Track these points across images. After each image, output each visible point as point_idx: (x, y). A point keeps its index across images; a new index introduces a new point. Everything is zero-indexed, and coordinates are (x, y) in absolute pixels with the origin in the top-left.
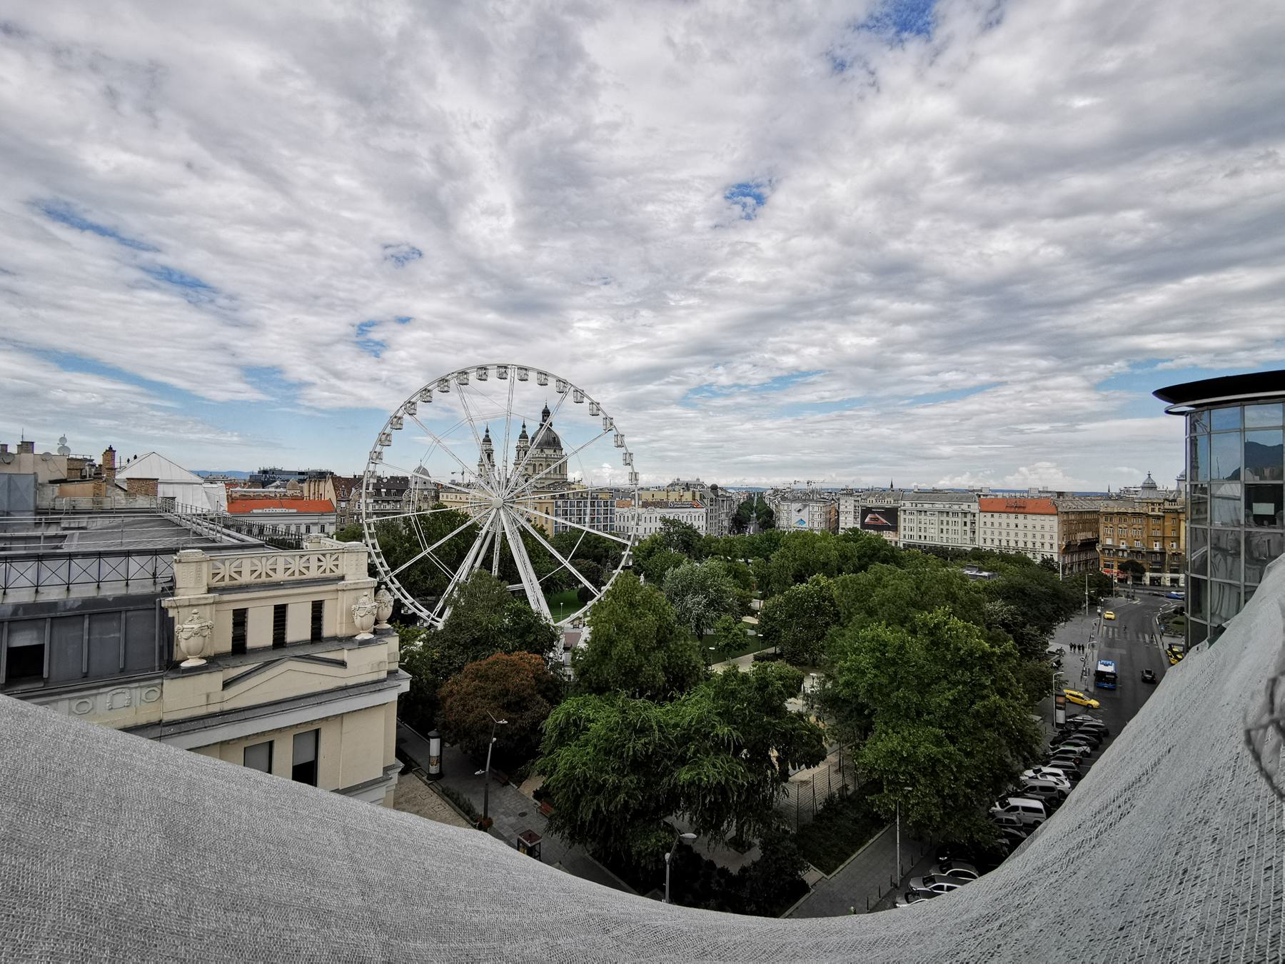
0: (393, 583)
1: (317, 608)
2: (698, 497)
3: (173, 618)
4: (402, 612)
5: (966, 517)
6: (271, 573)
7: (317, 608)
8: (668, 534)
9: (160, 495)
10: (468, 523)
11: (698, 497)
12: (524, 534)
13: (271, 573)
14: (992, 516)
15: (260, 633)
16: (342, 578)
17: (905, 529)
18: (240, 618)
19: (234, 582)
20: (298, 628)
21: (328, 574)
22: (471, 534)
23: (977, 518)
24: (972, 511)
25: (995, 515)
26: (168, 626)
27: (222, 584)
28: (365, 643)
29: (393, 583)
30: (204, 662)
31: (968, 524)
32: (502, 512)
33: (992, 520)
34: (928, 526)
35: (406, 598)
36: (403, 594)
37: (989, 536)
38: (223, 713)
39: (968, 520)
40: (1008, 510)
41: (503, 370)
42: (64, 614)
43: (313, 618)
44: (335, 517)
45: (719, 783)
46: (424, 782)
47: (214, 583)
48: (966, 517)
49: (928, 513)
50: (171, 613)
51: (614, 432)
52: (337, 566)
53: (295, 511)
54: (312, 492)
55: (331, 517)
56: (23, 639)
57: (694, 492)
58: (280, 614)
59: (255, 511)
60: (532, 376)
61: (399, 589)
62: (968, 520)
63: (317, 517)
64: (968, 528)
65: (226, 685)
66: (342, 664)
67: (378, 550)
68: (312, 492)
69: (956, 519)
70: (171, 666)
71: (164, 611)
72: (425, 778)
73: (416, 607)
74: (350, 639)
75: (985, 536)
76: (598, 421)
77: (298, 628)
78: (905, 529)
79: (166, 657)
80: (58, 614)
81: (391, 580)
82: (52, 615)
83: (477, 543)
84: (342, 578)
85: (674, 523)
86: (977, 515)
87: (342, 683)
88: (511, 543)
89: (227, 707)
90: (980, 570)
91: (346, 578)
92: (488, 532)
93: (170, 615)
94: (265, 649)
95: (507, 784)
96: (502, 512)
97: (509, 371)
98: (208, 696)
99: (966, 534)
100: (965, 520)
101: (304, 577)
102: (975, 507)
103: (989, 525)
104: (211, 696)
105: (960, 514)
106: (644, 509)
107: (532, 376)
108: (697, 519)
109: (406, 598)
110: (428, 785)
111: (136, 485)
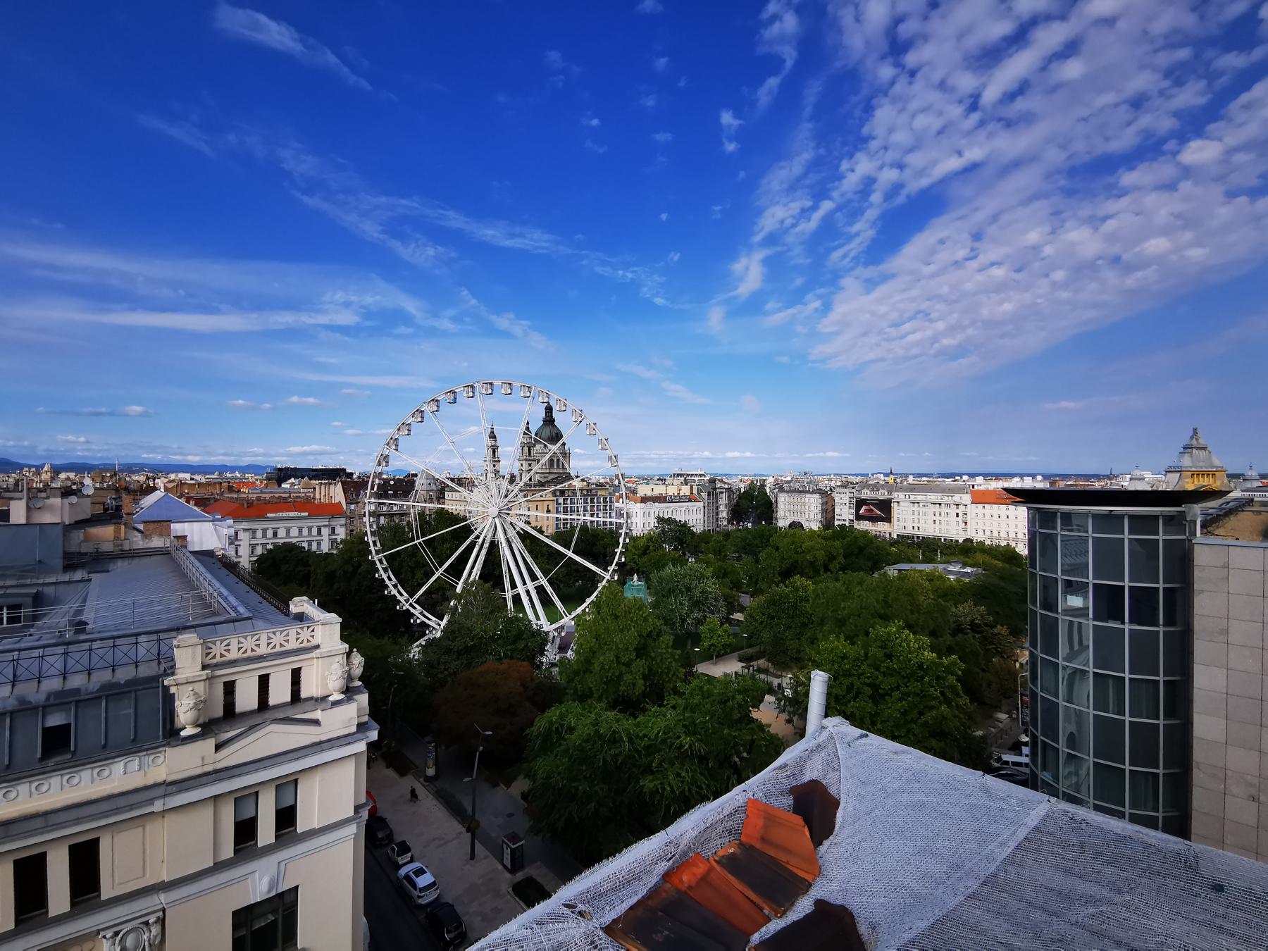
1: (296, 675)
2: (695, 491)
3: (174, 694)
6: (255, 648)
7: (296, 675)
8: (663, 532)
9: (173, 534)
11: (695, 491)
13: (255, 648)
14: (984, 507)
15: (247, 698)
16: (318, 647)
17: (898, 521)
18: (230, 688)
19: (223, 659)
20: (280, 693)
21: (305, 644)
26: (169, 700)
27: (214, 661)
28: (336, 703)
30: (199, 730)
32: (497, 520)
33: (984, 511)
34: (920, 517)
38: (216, 772)
40: (1000, 501)
42: (87, 697)
43: (293, 684)
45: (682, 792)
46: (421, 783)
47: (208, 661)
49: (921, 504)
50: (173, 690)
52: (313, 636)
53: (306, 514)
54: (323, 494)
56: (55, 720)
57: (692, 487)
58: (264, 681)
59: (269, 515)
63: (328, 520)
64: (960, 519)
65: (218, 747)
66: (316, 722)
68: (323, 494)
69: (948, 511)
70: (172, 734)
71: (166, 689)
72: (422, 780)
74: (324, 698)
77: (280, 693)
78: (898, 521)
79: (168, 727)
80: (82, 698)
82: (77, 698)
84: (318, 647)
85: (670, 521)
87: (317, 739)
89: (219, 766)
91: (321, 646)
93: (172, 692)
94: (251, 713)
95: (496, 785)
98: (203, 759)
99: (958, 525)
101: (283, 649)
102: (967, 498)
103: (980, 515)
104: (205, 758)
108: (694, 516)
110: (424, 786)
111: (152, 526)
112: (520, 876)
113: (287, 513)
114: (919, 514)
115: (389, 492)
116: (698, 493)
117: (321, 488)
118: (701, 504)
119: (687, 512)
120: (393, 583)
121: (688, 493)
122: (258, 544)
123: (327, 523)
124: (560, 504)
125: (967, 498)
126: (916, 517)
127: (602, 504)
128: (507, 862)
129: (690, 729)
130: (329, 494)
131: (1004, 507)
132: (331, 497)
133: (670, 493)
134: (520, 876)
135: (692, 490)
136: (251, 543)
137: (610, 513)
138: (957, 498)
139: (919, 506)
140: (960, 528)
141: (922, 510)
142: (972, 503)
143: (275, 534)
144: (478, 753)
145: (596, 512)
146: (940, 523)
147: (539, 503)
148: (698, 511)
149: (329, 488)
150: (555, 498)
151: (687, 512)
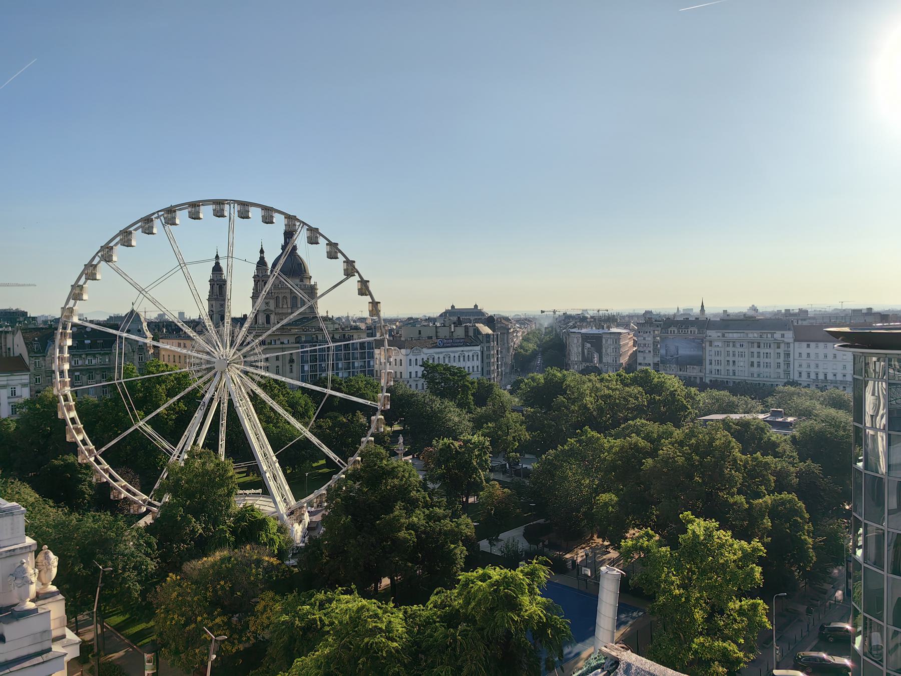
0: (99, 463)
4: (112, 497)
5: (779, 347)
10: (187, 390)
12: (254, 397)
14: (808, 346)
17: (711, 364)
22: (193, 400)
24: (786, 340)
25: (812, 345)
29: (99, 463)
31: (782, 355)
33: (808, 351)
34: (736, 359)
35: (116, 480)
36: (111, 476)
37: (804, 370)
39: (781, 351)
41: (218, 207)
44: (27, 377)
48: (779, 347)
49: (738, 345)
51: (356, 278)
55: (23, 377)
60: (256, 214)
61: (106, 471)
62: (781, 351)
63: (5, 378)
64: (781, 360)
67: (81, 426)
73: (128, 491)
75: (800, 369)
76: (339, 265)
78: (711, 364)
81: (96, 460)
83: (198, 415)
86: (792, 345)
88: (241, 411)
92: (212, 399)
97: (227, 207)
99: (779, 367)
100: (778, 351)
102: (789, 336)
103: (804, 356)
105: (772, 345)
106: (409, 351)
107: (256, 214)
109: (116, 480)
114: (734, 355)
115: (86, 342)
118: (478, 348)
119: (462, 359)
123: (5, 383)
126: (731, 359)
130: (5, 345)
132: (9, 349)
137: (369, 362)
138: (778, 335)
139: (734, 346)
140: (781, 371)
141: (739, 349)
142: (795, 341)
144: (210, 663)
146: (759, 366)
148: (475, 358)
149: (5, 338)
151: (462, 359)
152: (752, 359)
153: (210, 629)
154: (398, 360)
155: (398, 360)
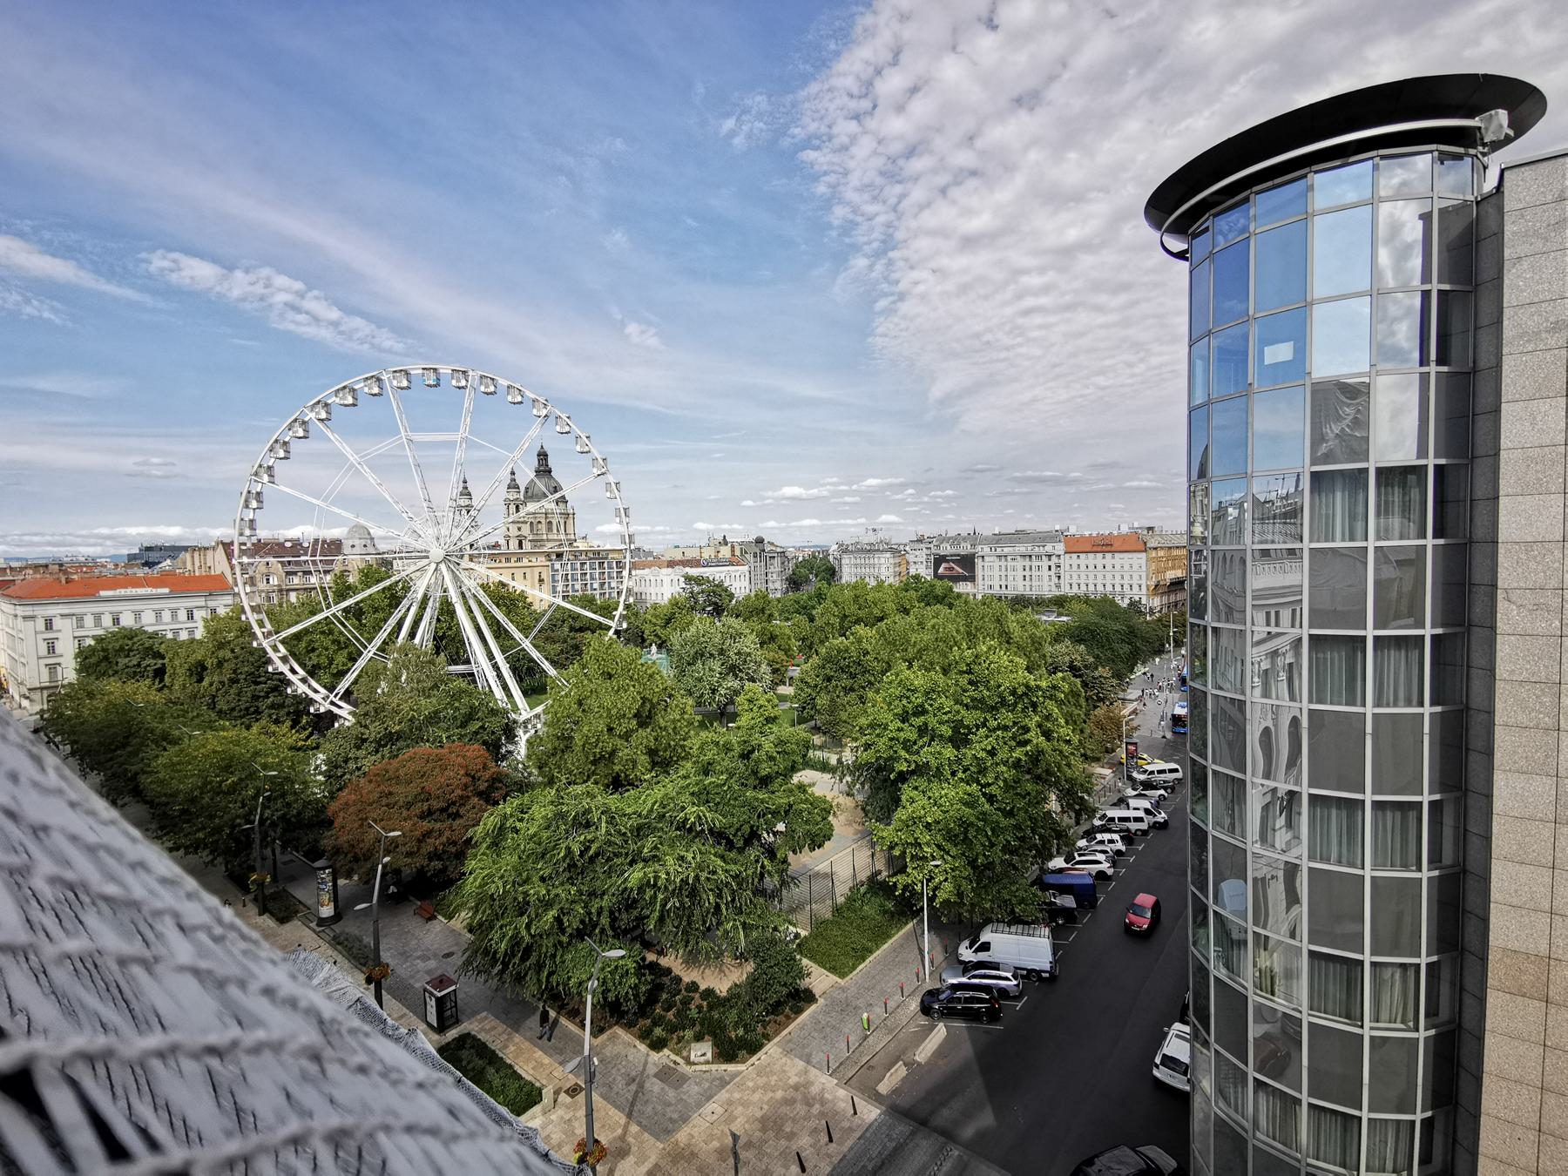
2: (738, 553)
8: (693, 595)
11: (738, 553)
23: (1062, 561)
32: (443, 567)
33: (1079, 562)
35: (316, 691)
39: (1051, 563)
40: (1095, 549)
45: (684, 882)
46: (314, 931)
49: (1009, 558)
53: (166, 590)
54: (197, 564)
57: (733, 547)
59: (103, 593)
61: (304, 680)
68: (197, 564)
69: (1040, 564)
72: (313, 925)
85: (698, 580)
90: (1060, 615)
95: (432, 918)
96: (443, 567)
102: (1060, 548)
105: (1044, 557)
106: (670, 569)
108: (739, 583)
110: (317, 933)
112: (452, 1034)
113: (134, 590)
116: (742, 555)
117: (193, 557)
118: (746, 568)
120: (281, 655)
121: (728, 555)
122: (88, 636)
123: (203, 604)
124: (557, 570)
125: (1060, 548)
127: (615, 570)
128: (433, 1018)
129: (703, 796)
131: (1100, 555)
133: (705, 556)
134: (452, 1034)
135: (733, 551)
136: (76, 634)
138: (1049, 548)
139: (1006, 560)
140: (1052, 584)
143: (116, 621)
144: (380, 866)
145: (607, 581)
147: (527, 570)
148: (742, 577)
149: (205, 555)
150: (549, 563)
152: (1025, 573)
153: (375, 821)
154: (659, 581)
155: (659, 581)
